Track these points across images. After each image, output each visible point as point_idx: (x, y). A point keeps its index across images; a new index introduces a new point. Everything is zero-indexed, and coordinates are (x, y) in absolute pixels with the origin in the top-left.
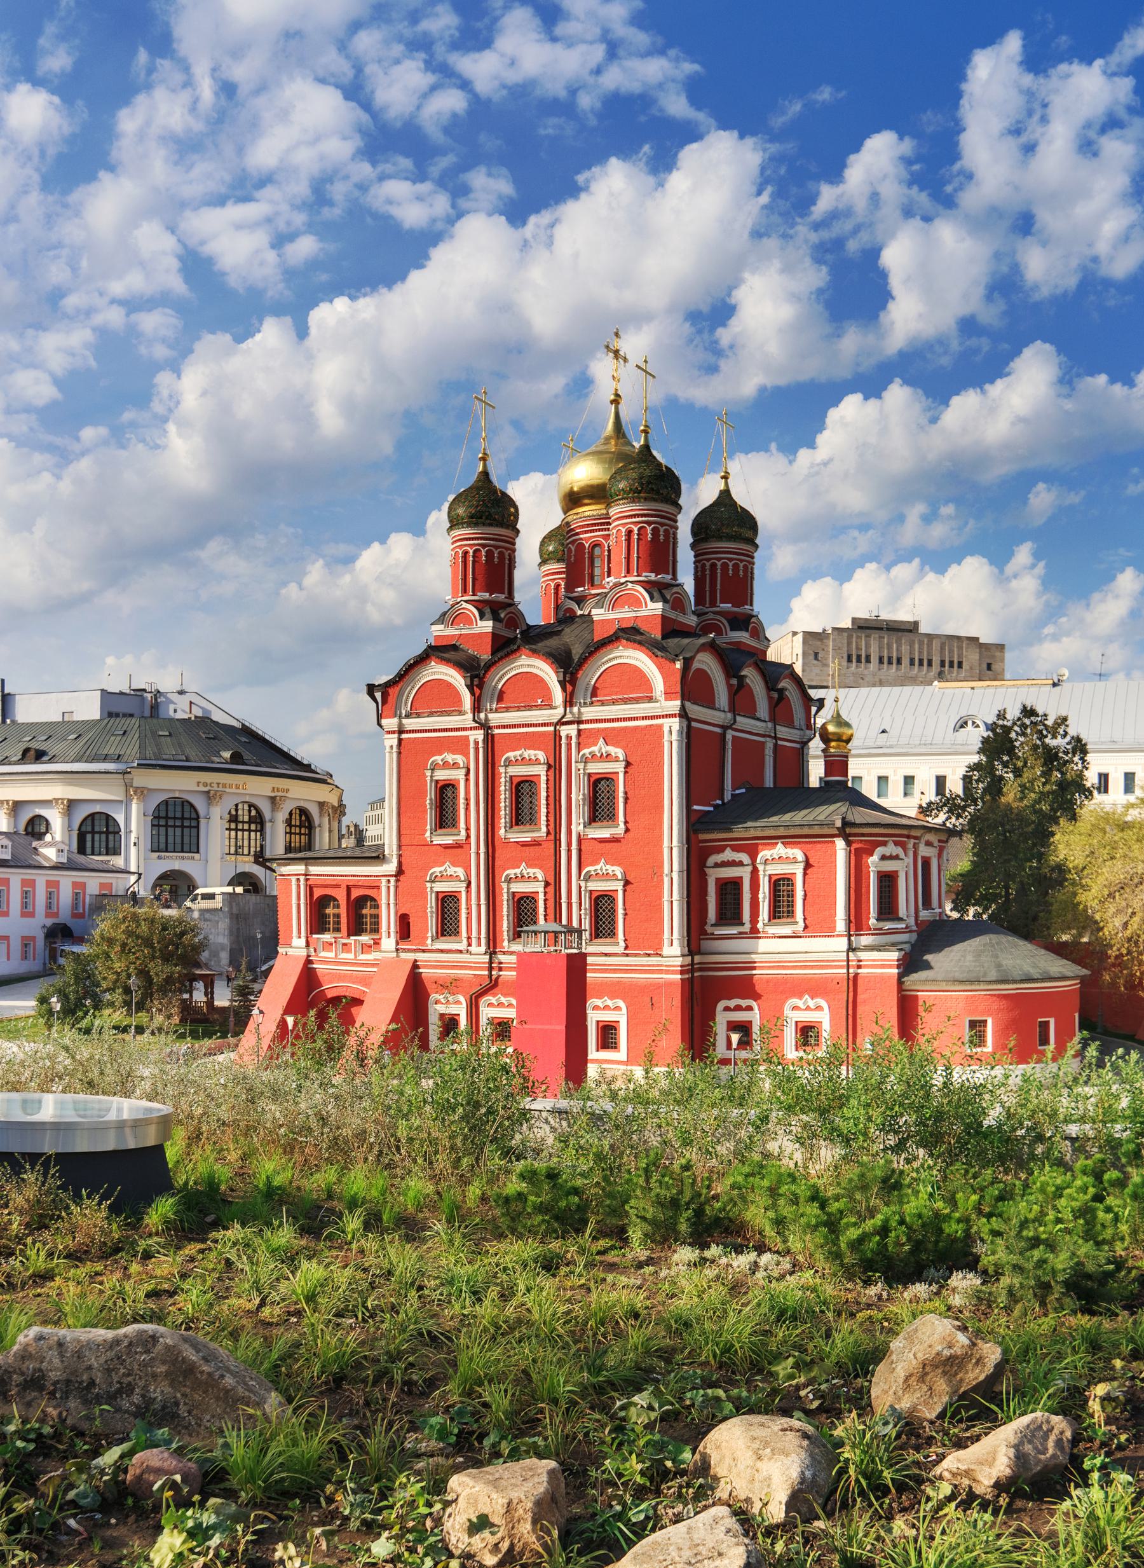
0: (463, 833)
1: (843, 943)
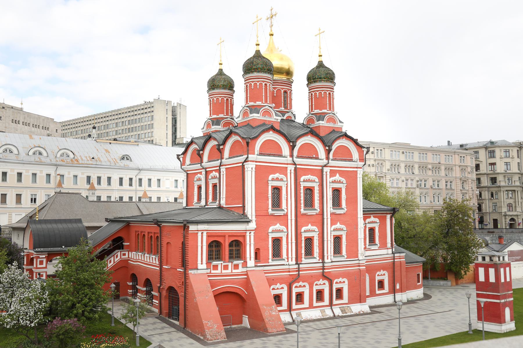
0: (286, 210)
1: (390, 251)
